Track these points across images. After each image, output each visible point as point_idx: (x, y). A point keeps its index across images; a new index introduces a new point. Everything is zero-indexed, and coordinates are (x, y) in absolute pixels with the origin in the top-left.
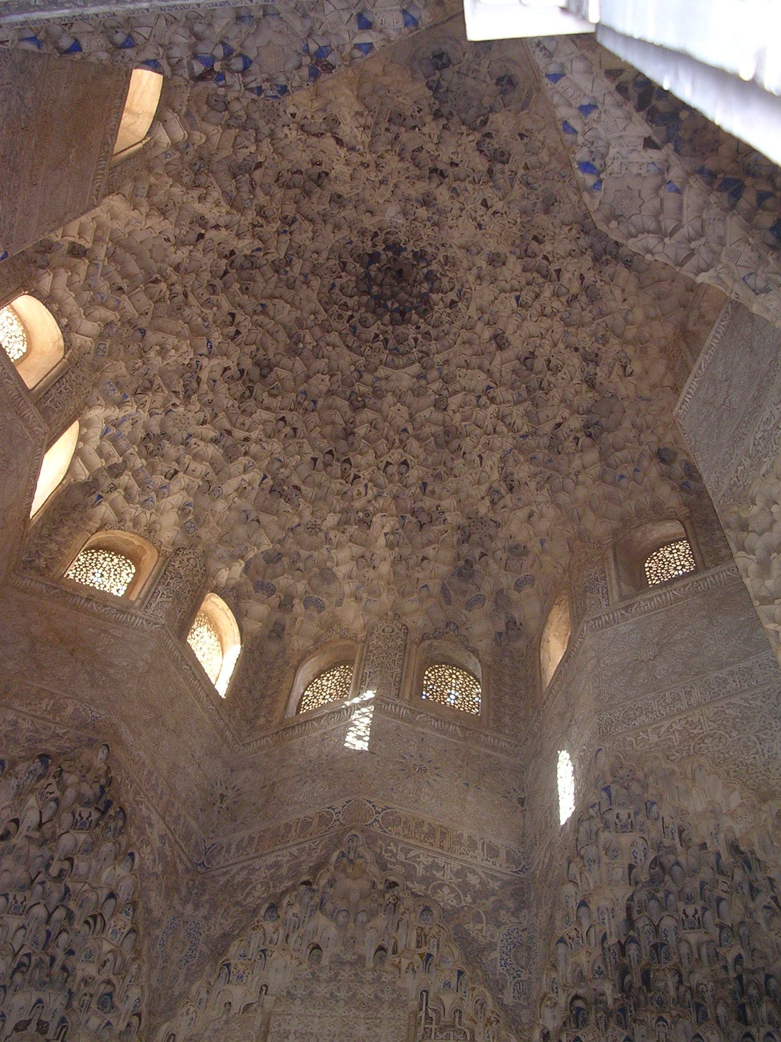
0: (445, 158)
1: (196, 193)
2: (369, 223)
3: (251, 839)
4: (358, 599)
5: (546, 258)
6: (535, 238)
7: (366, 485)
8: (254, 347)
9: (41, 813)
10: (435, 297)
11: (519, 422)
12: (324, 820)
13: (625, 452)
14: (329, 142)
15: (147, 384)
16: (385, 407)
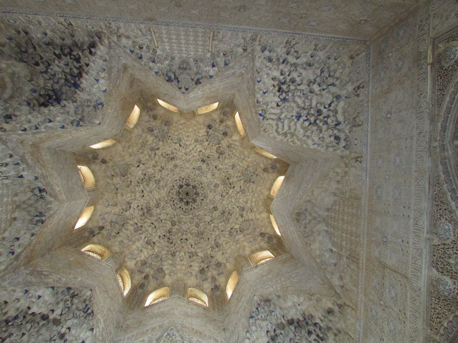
0: (207, 155)
1: (141, 151)
2: (183, 175)
3: (133, 336)
4: (170, 276)
5: (230, 184)
6: (228, 179)
7: (175, 245)
8: (147, 201)
9: (62, 310)
10: (197, 198)
11: (220, 228)
12: (160, 326)
13: (250, 235)
14: (178, 145)
15: (115, 204)
16: (181, 226)
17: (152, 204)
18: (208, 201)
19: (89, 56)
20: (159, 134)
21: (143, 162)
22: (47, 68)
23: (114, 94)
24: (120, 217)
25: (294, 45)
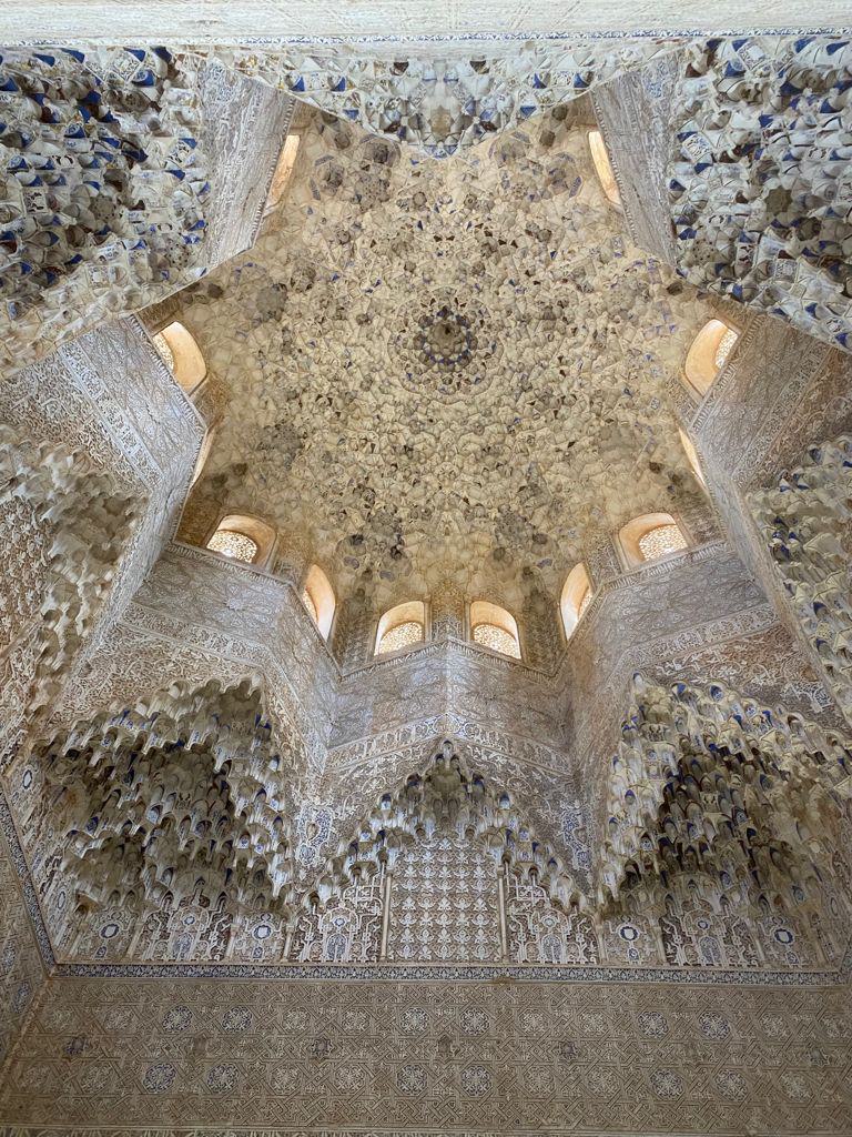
0: (400, 475)
1: (563, 494)
7: (470, 225)
9: (759, 242)
10: (419, 329)
11: (342, 284)
14: (472, 502)
17: (537, 331)
18: (387, 334)
19: (638, 861)
20: (520, 524)
21: (560, 455)
22: (734, 817)
23: (602, 731)
24: (623, 306)
25: (212, 928)
